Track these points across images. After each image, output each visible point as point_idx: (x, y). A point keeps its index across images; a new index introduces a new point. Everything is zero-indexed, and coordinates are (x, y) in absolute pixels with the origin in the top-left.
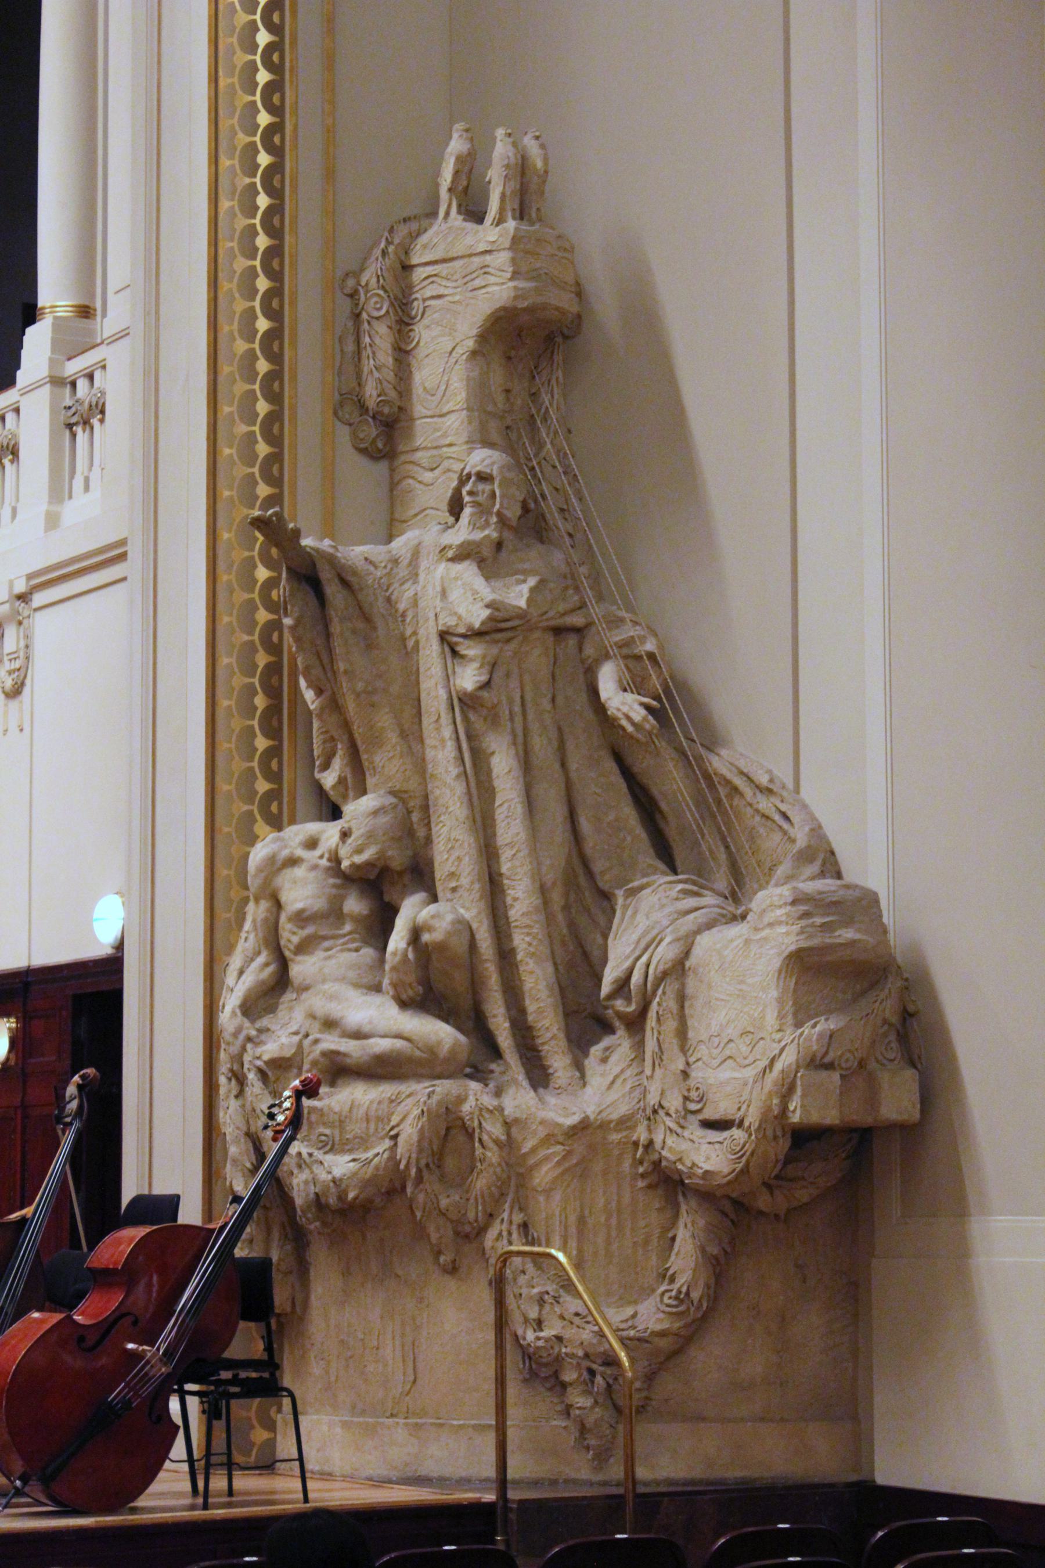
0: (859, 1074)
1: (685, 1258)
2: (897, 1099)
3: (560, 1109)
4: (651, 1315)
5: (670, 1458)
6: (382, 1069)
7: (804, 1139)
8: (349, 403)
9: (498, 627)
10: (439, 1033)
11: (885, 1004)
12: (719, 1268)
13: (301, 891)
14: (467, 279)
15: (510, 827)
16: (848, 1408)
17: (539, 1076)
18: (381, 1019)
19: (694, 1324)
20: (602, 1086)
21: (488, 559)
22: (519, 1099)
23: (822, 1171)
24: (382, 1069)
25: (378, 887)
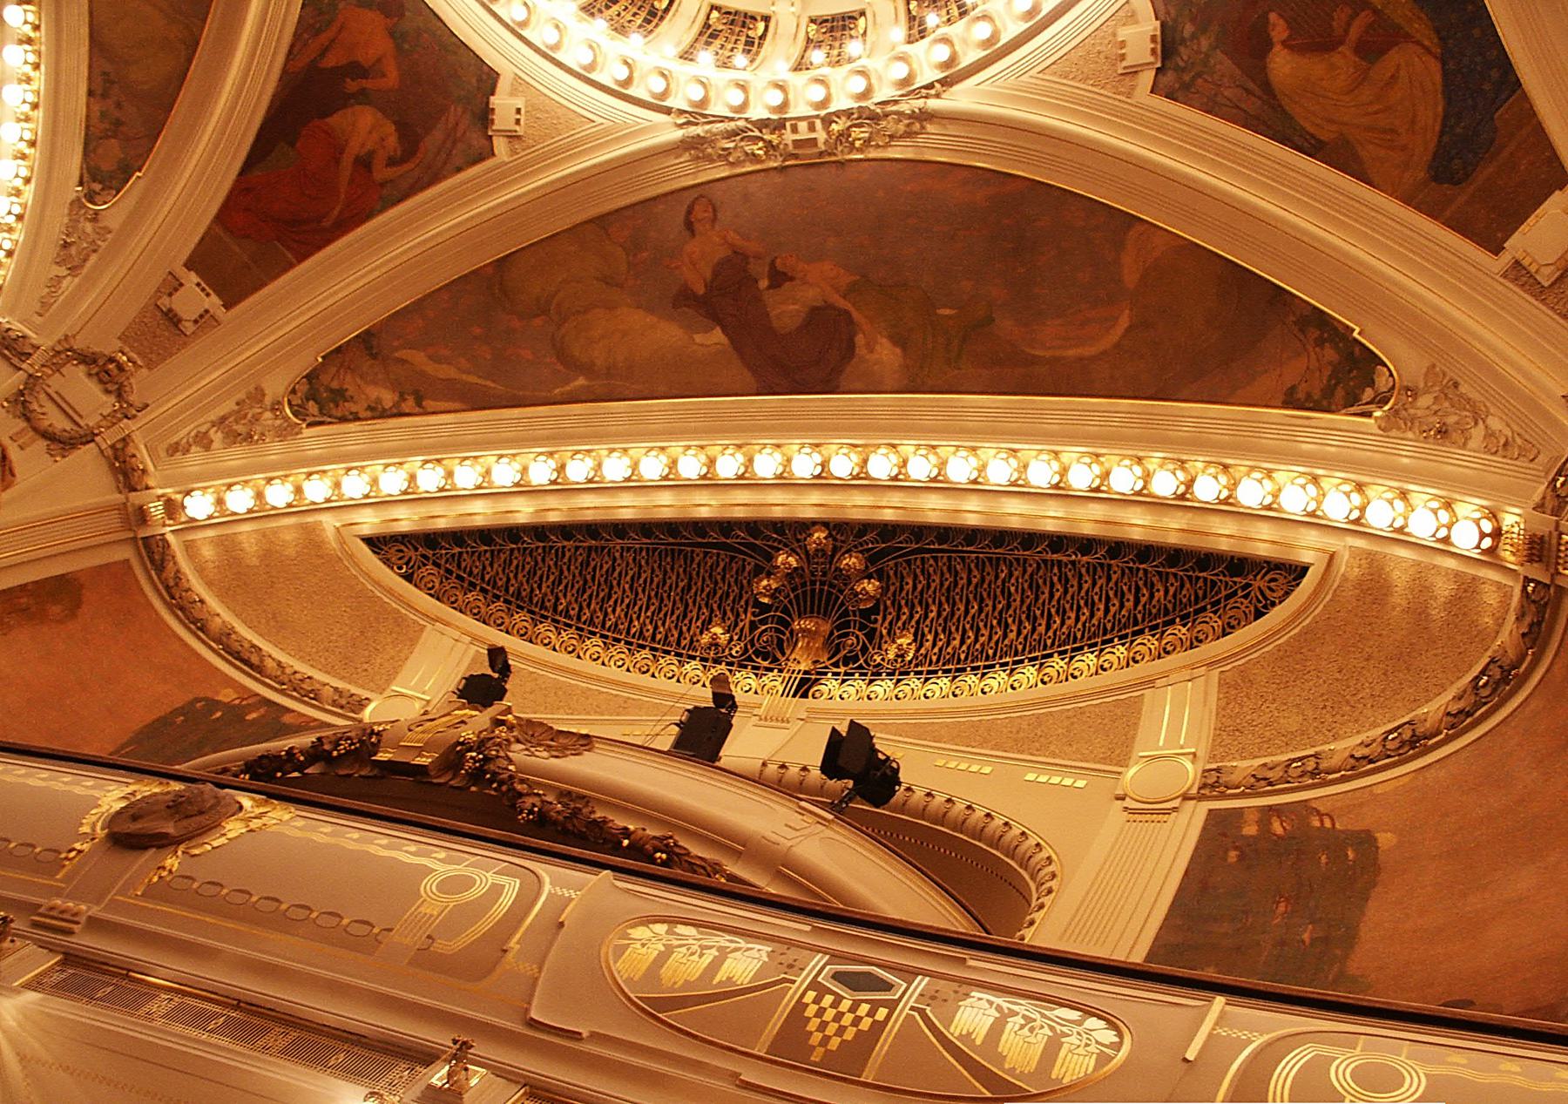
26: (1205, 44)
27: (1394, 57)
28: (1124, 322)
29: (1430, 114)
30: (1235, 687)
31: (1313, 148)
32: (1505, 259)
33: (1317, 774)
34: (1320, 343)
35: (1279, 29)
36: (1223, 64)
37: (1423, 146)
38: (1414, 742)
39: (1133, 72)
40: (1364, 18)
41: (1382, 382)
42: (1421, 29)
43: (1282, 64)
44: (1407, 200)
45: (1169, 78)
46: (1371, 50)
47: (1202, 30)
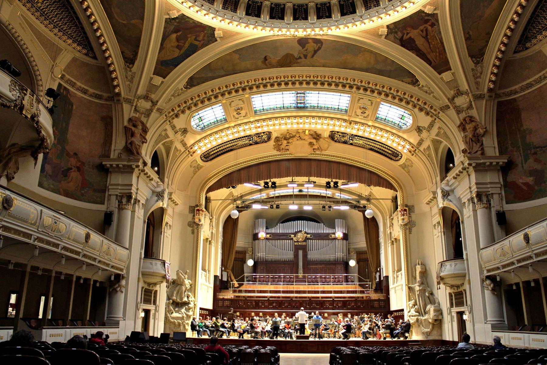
0: (438, 316)
1: (431, 327)
2: (440, 317)
3: (424, 318)
4: (429, 330)
5: (431, 338)
6: (415, 316)
7: (436, 320)
8: (412, 276)
9: (419, 290)
10: (417, 314)
11: (440, 312)
12: (433, 328)
13: (411, 305)
14: (419, 269)
15: (421, 302)
16: (441, 335)
17: (423, 316)
18: (415, 313)
19: (432, 330)
20: (426, 317)
21: (419, 286)
22: (422, 318)
23: (438, 322)
24: (415, 316)
25: (415, 305)
26: (176, 24)
27: (177, 50)
28: (125, 22)
29: (171, 57)
30: (74, 60)
31: (162, 44)
32: (152, 76)
33: (73, 85)
34: (133, 54)
35: (179, 34)
36: (172, 28)
37: (166, 58)
38: (85, 92)
39: (168, 14)
40: (182, 45)
41: (131, 66)
42: (182, 52)
43: (174, 36)
44: (157, 60)
45: (169, 20)
46: (178, 47)
47: (178, 23)
